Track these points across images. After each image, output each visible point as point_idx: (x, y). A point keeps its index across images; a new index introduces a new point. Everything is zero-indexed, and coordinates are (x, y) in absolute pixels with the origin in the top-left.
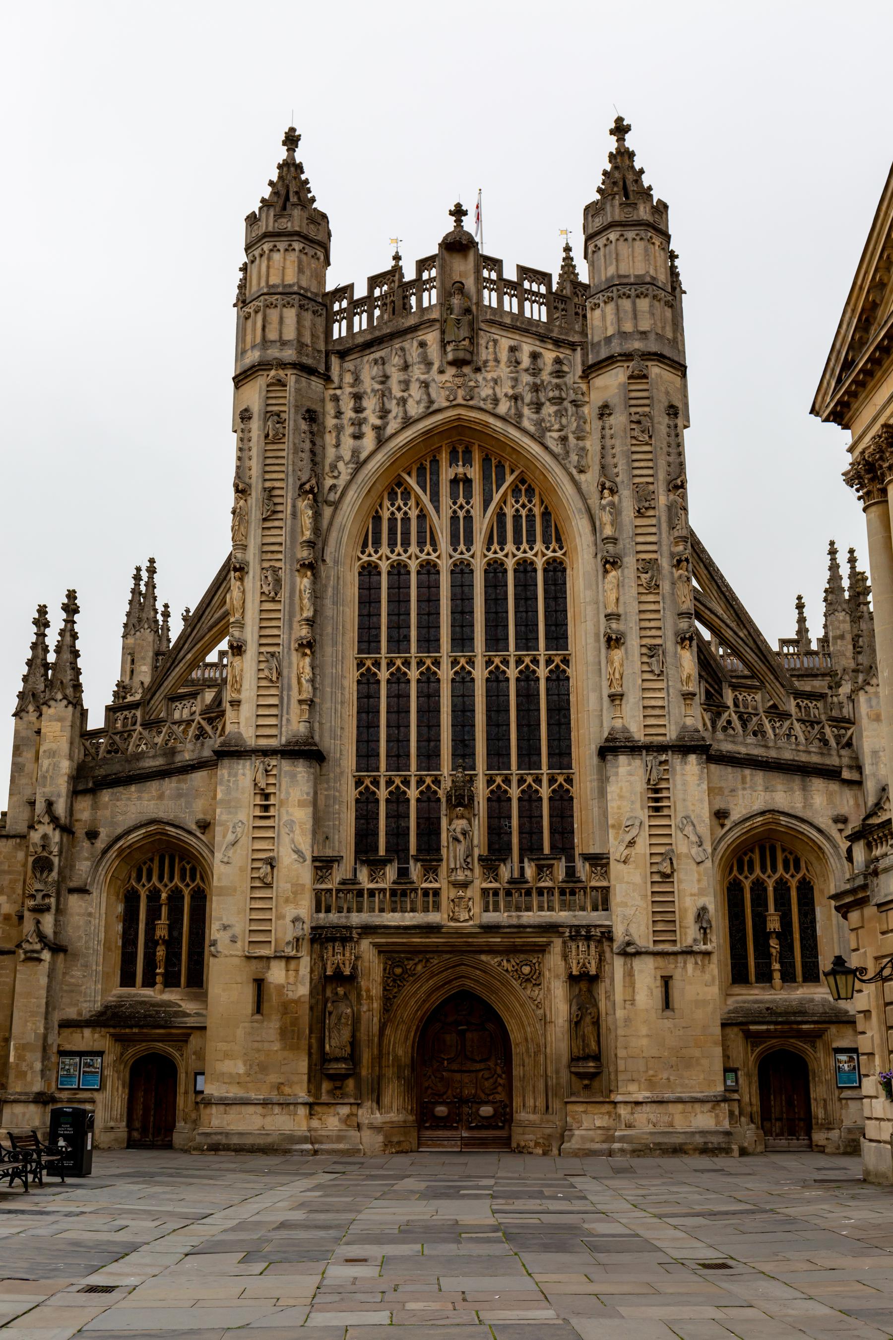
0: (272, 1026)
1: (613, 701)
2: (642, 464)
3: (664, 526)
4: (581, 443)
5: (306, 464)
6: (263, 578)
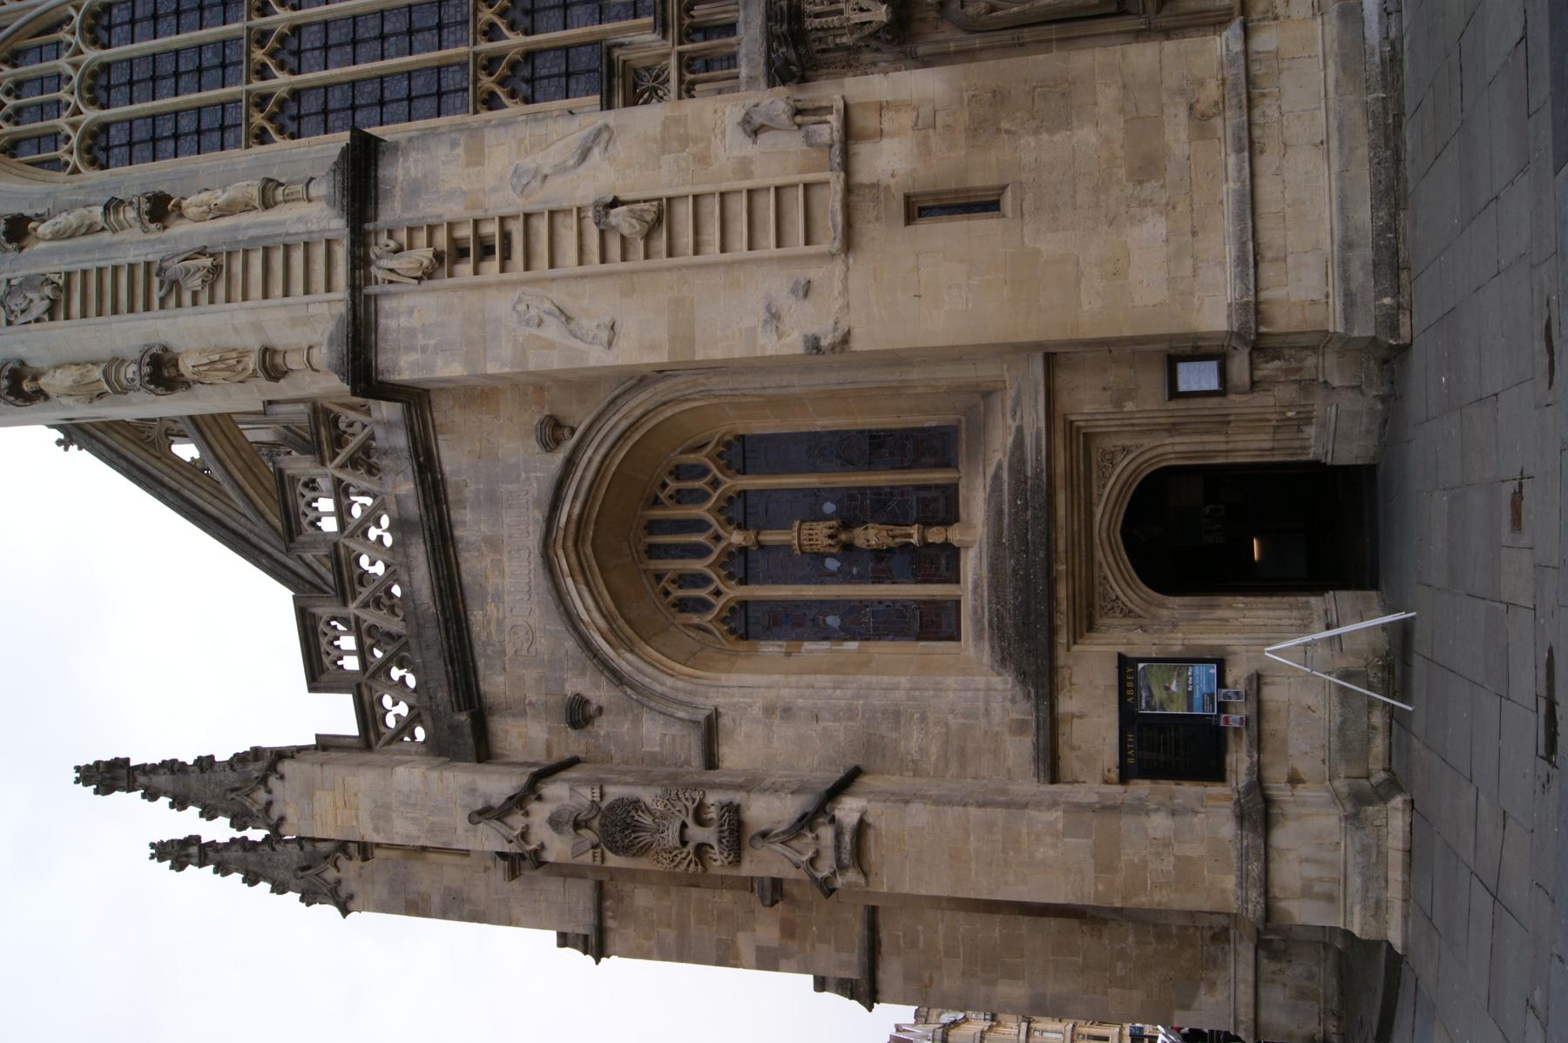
6: (22, 319)
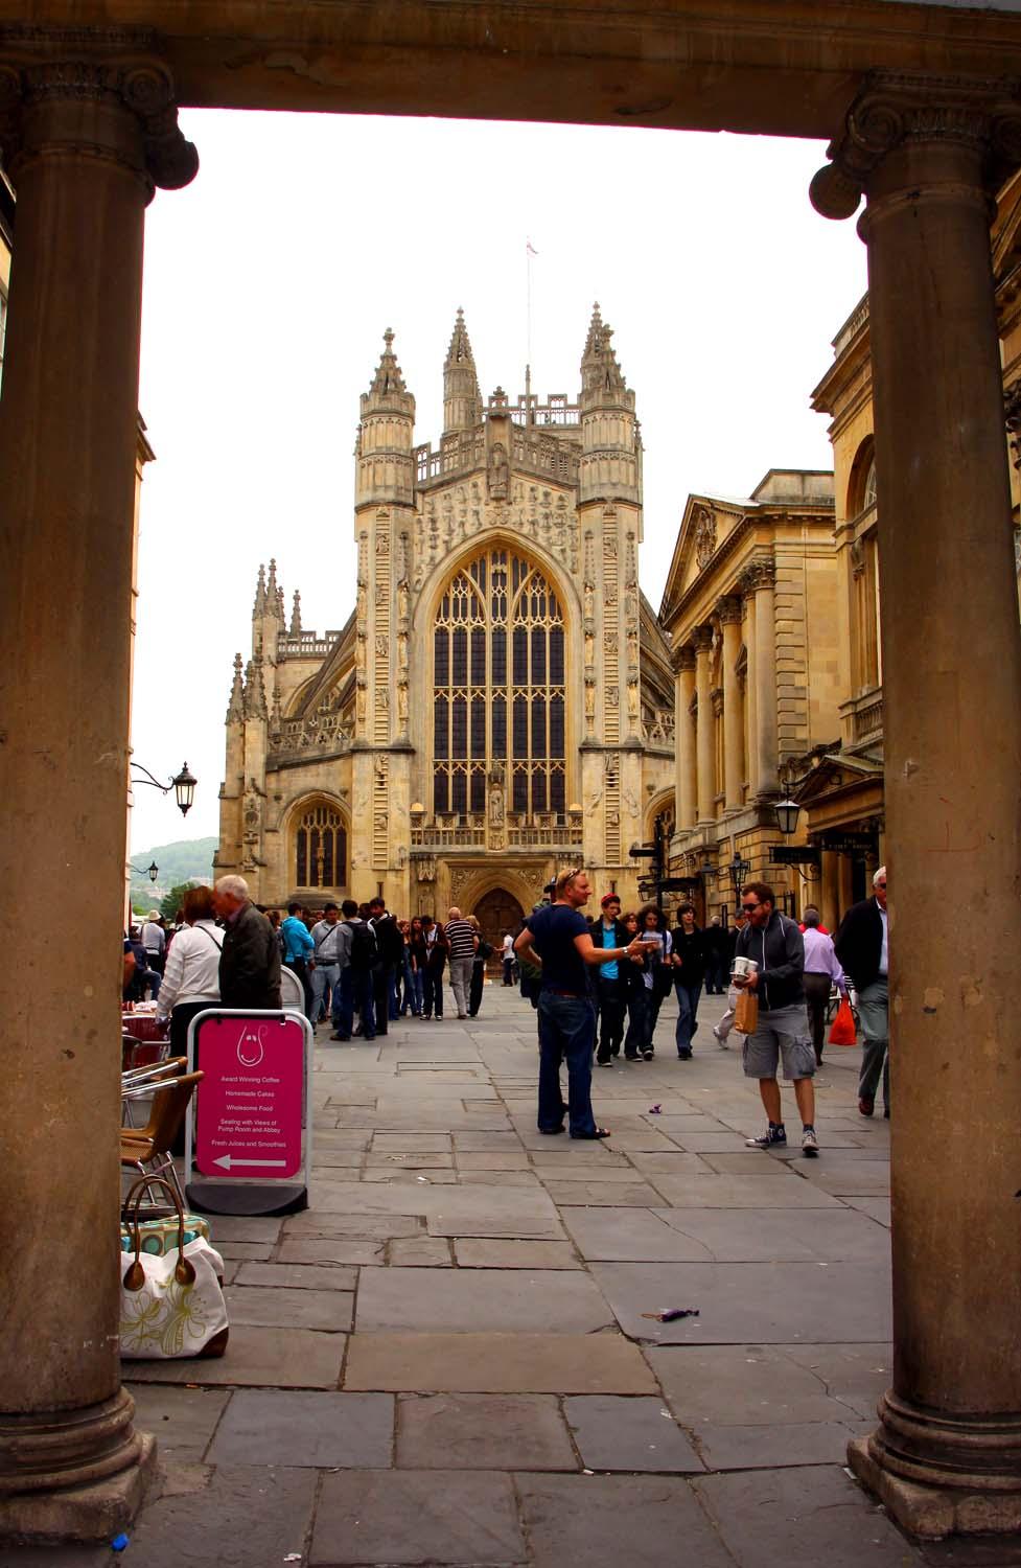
2: (610, 572)
3: (622, 611)
4: (574, 554)
5: (402, 569)
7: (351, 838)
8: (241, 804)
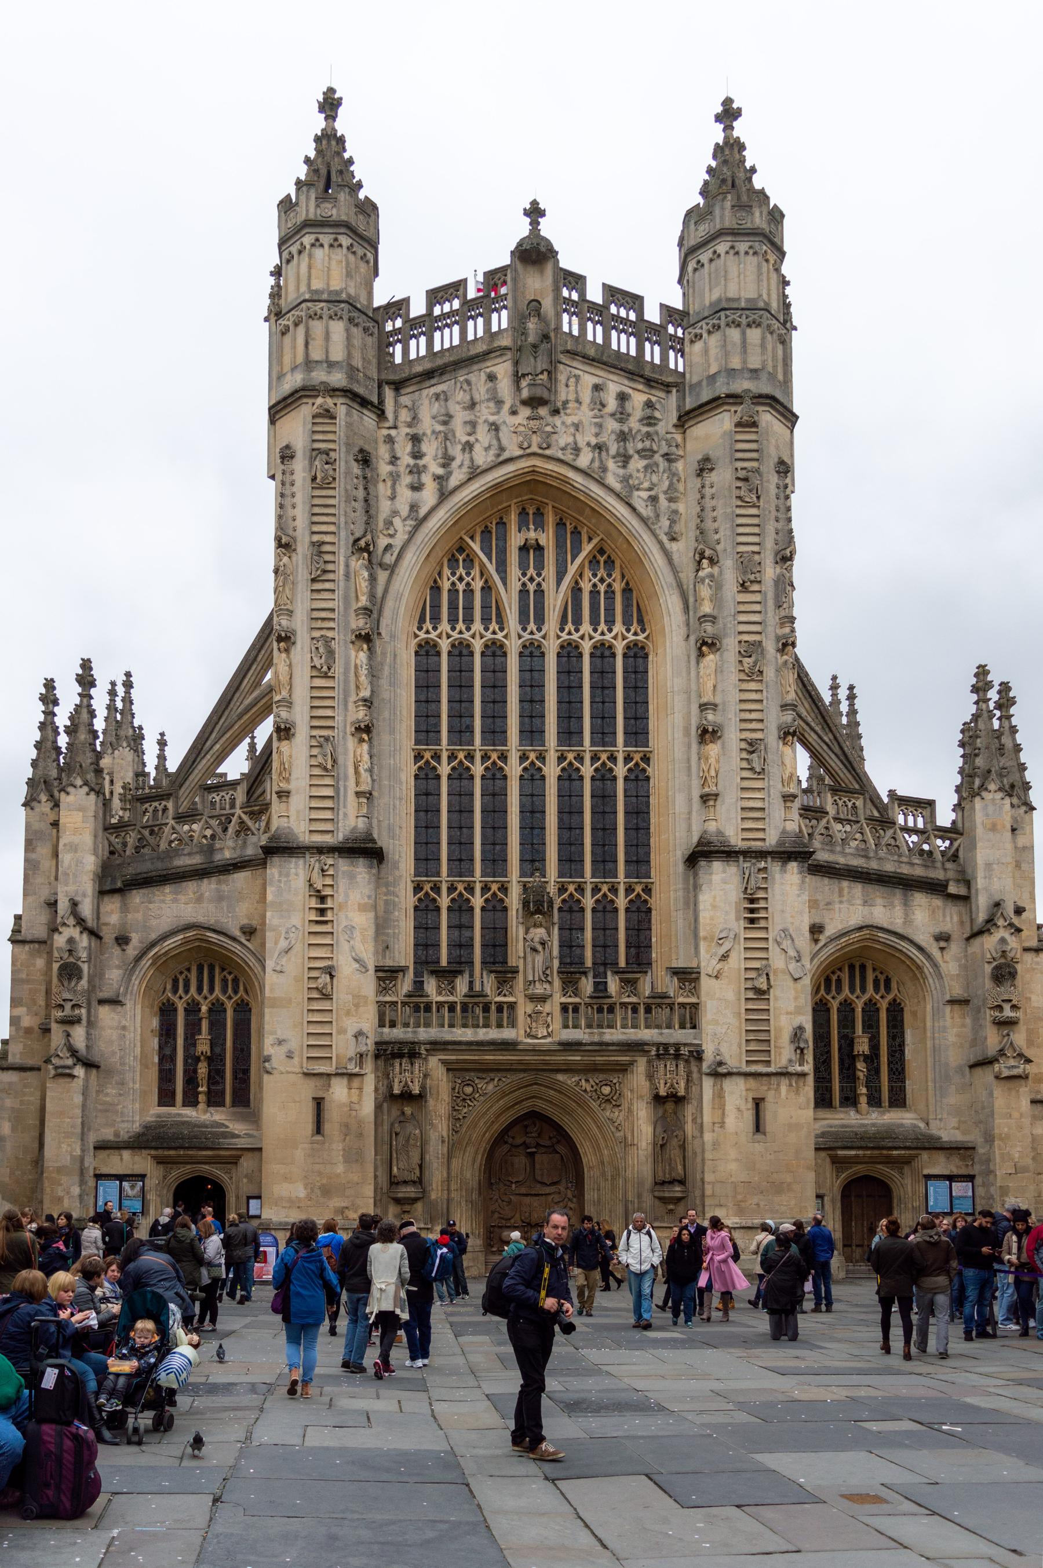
0: (337, 1147)
1: (705, 802)
4: (673, 506)
7: (262, 1015)
8: (50, 953)
